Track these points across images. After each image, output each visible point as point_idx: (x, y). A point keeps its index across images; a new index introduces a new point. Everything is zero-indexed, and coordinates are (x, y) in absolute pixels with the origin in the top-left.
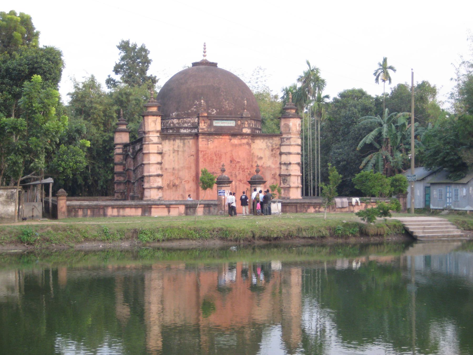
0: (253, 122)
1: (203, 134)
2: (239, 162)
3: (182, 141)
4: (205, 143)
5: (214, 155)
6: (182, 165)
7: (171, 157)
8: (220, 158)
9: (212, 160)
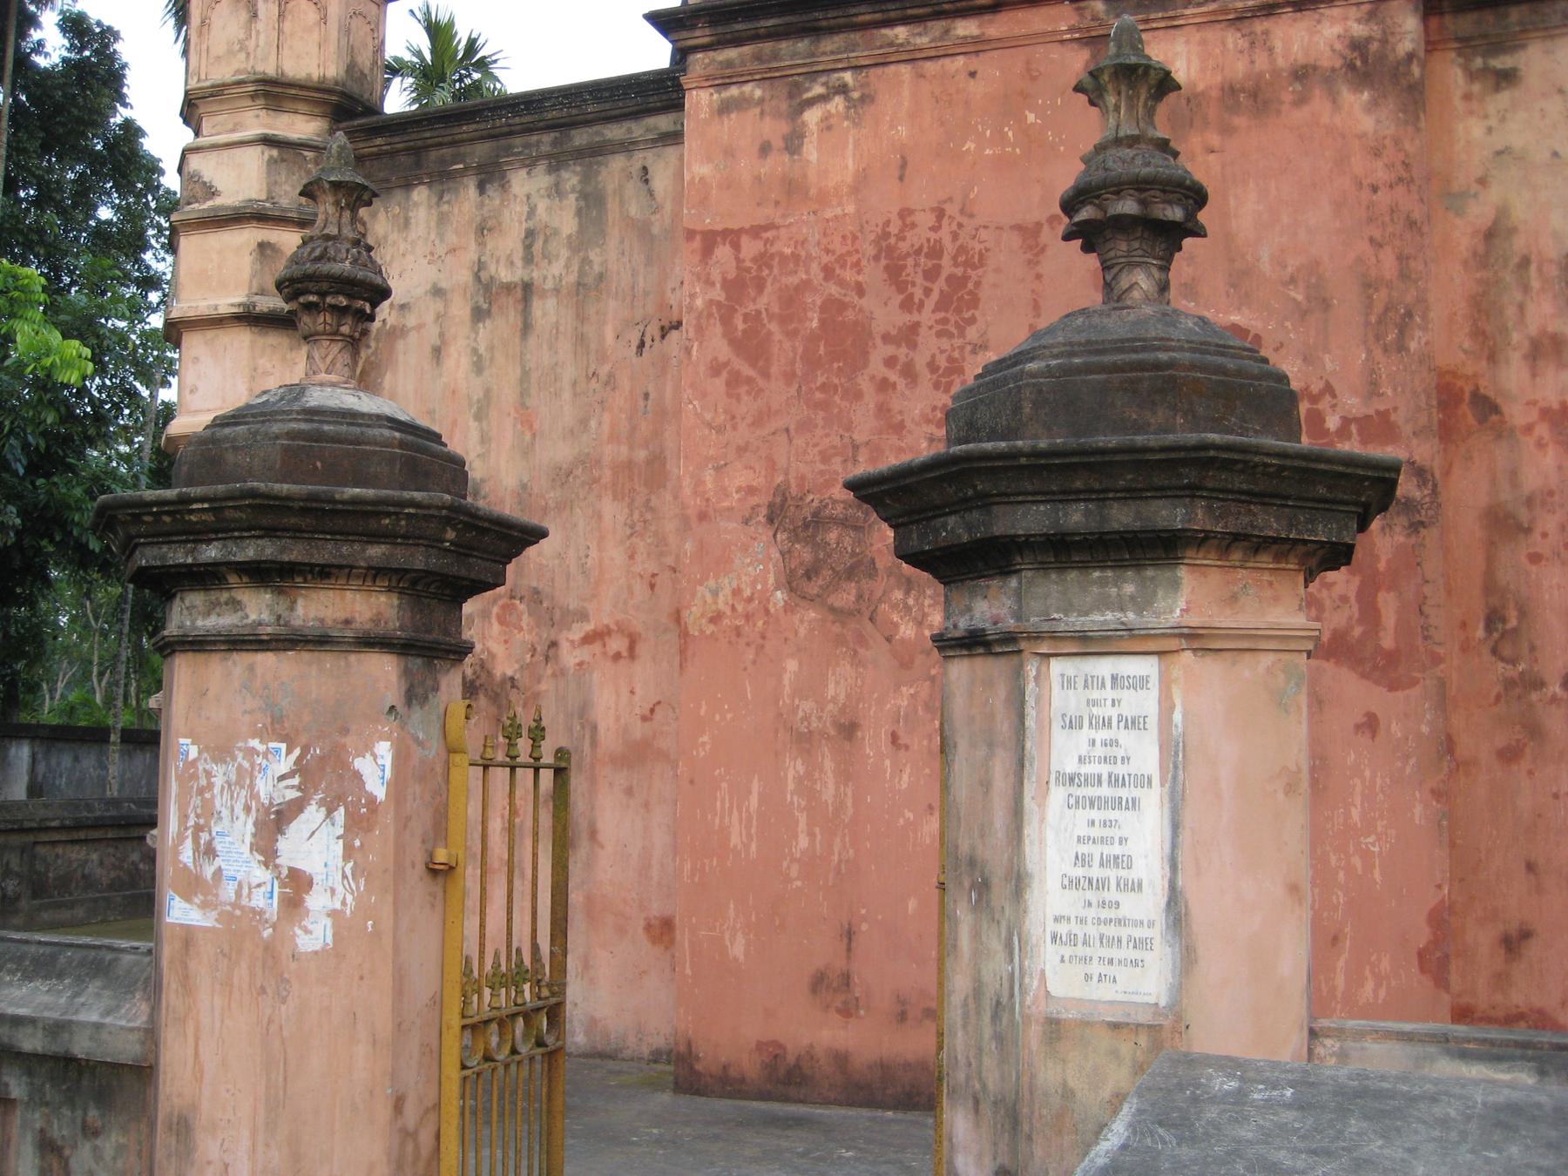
3: (571, 178)
5: (873, 275)
6: (559, 452)
7: (458, 361)
9: (843, 340)
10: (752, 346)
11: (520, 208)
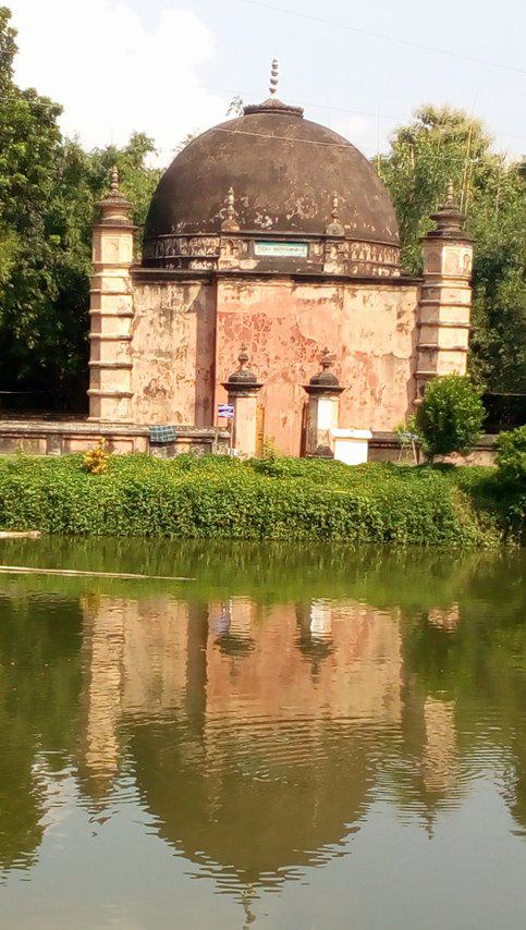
0: (367, 248)
1: (231, 275)
2: (311, 342)
4: (230, 293)
8: (267, 329)
11: (170, 294)
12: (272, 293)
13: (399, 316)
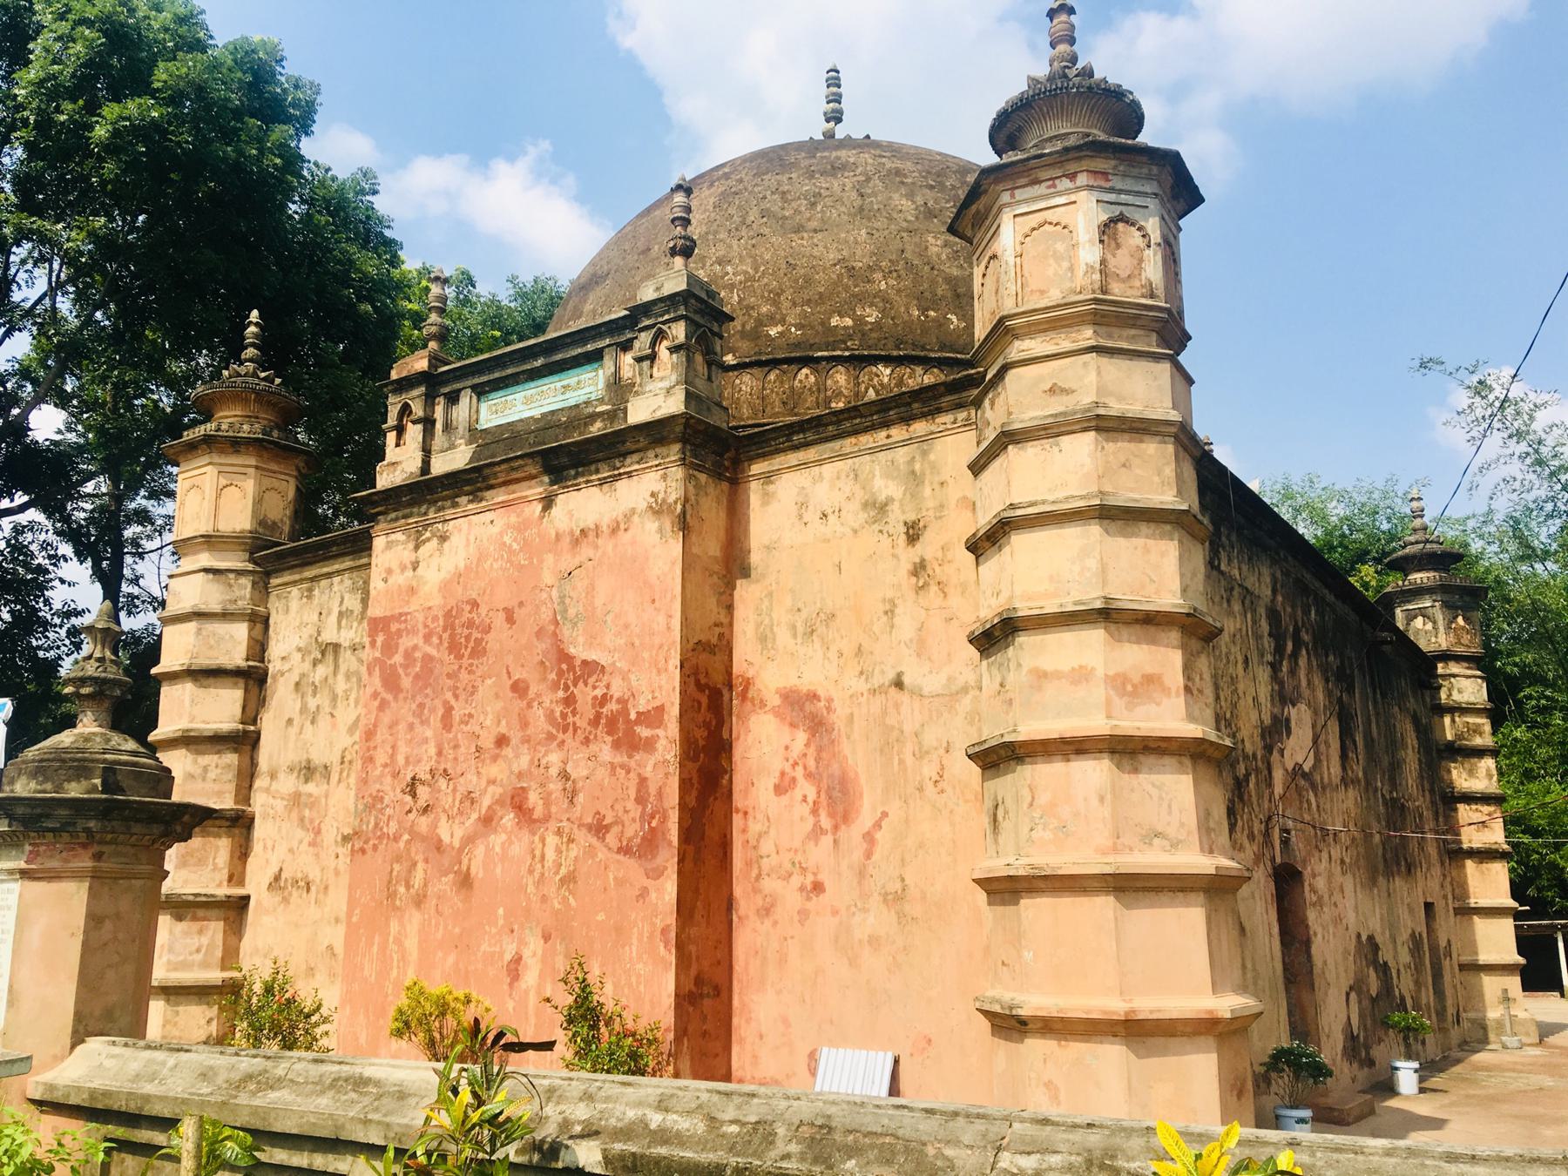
2: (591, 668)
8: (478, 651)
10: (391, 682)
12: (495, 530)
13: (913, 533)
